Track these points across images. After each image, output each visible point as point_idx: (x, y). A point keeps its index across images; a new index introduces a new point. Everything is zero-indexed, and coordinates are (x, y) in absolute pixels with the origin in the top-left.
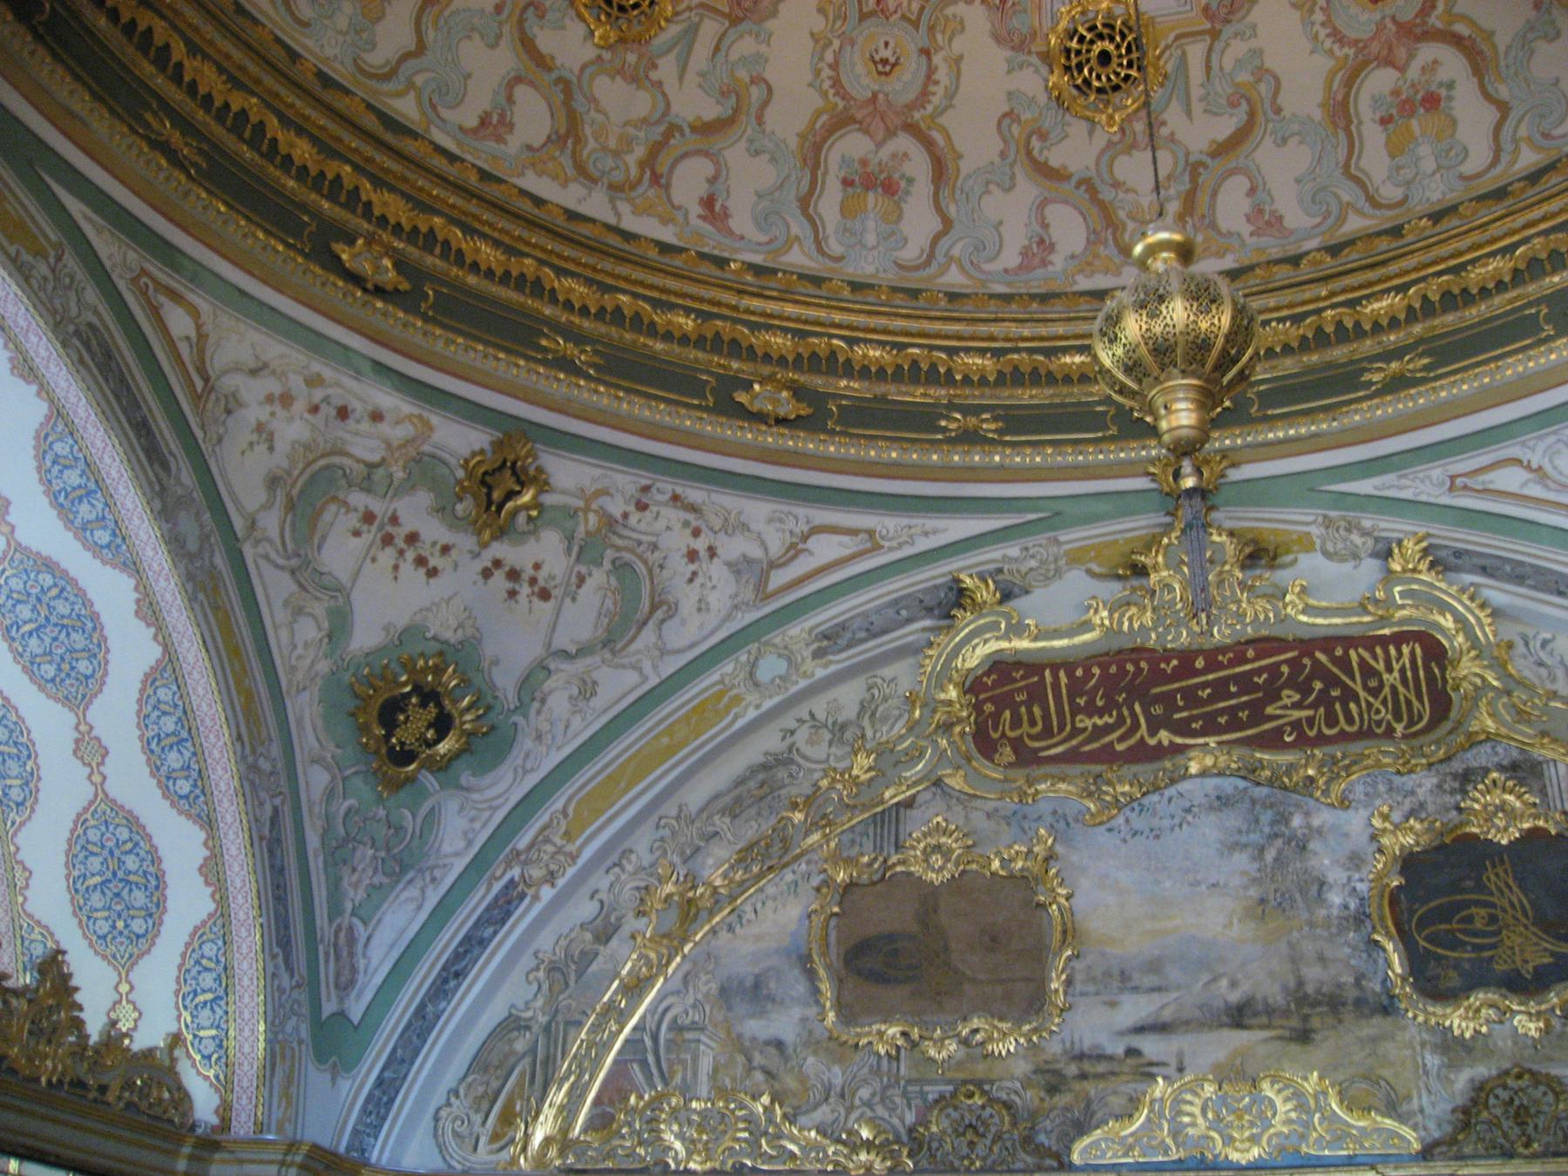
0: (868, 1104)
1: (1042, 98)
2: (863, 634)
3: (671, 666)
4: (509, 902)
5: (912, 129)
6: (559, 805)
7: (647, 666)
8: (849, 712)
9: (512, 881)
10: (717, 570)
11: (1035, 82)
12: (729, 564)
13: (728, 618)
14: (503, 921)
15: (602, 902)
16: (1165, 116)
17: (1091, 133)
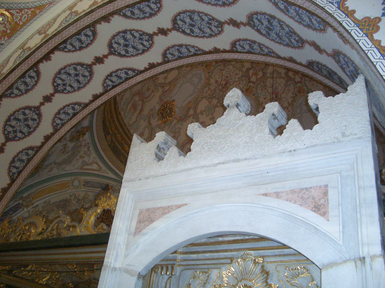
0: (64, 276)
1: (157, 111)
2: (91, 186)
3: (63, 172)
4: (17, 208)
5: (143, 101)
6: (34, 191)
7: (60, 170)
8: (81, 198)
9: (20, 203)
10: (81, 160)
11: (158, 107)
12: (83, 161)
13: (75, 169)
14: (15, 212)
15: (30, 215)
16: (166, 127)
17: (157, 121)
